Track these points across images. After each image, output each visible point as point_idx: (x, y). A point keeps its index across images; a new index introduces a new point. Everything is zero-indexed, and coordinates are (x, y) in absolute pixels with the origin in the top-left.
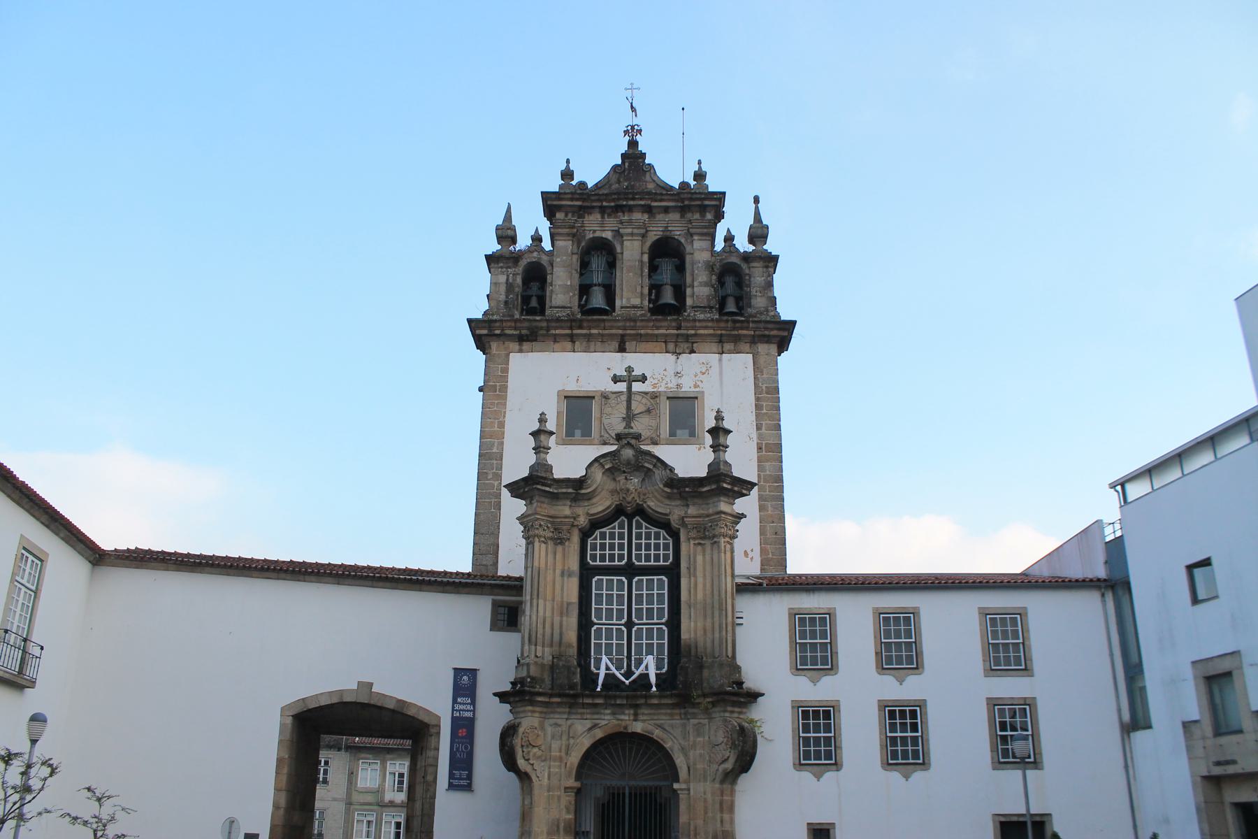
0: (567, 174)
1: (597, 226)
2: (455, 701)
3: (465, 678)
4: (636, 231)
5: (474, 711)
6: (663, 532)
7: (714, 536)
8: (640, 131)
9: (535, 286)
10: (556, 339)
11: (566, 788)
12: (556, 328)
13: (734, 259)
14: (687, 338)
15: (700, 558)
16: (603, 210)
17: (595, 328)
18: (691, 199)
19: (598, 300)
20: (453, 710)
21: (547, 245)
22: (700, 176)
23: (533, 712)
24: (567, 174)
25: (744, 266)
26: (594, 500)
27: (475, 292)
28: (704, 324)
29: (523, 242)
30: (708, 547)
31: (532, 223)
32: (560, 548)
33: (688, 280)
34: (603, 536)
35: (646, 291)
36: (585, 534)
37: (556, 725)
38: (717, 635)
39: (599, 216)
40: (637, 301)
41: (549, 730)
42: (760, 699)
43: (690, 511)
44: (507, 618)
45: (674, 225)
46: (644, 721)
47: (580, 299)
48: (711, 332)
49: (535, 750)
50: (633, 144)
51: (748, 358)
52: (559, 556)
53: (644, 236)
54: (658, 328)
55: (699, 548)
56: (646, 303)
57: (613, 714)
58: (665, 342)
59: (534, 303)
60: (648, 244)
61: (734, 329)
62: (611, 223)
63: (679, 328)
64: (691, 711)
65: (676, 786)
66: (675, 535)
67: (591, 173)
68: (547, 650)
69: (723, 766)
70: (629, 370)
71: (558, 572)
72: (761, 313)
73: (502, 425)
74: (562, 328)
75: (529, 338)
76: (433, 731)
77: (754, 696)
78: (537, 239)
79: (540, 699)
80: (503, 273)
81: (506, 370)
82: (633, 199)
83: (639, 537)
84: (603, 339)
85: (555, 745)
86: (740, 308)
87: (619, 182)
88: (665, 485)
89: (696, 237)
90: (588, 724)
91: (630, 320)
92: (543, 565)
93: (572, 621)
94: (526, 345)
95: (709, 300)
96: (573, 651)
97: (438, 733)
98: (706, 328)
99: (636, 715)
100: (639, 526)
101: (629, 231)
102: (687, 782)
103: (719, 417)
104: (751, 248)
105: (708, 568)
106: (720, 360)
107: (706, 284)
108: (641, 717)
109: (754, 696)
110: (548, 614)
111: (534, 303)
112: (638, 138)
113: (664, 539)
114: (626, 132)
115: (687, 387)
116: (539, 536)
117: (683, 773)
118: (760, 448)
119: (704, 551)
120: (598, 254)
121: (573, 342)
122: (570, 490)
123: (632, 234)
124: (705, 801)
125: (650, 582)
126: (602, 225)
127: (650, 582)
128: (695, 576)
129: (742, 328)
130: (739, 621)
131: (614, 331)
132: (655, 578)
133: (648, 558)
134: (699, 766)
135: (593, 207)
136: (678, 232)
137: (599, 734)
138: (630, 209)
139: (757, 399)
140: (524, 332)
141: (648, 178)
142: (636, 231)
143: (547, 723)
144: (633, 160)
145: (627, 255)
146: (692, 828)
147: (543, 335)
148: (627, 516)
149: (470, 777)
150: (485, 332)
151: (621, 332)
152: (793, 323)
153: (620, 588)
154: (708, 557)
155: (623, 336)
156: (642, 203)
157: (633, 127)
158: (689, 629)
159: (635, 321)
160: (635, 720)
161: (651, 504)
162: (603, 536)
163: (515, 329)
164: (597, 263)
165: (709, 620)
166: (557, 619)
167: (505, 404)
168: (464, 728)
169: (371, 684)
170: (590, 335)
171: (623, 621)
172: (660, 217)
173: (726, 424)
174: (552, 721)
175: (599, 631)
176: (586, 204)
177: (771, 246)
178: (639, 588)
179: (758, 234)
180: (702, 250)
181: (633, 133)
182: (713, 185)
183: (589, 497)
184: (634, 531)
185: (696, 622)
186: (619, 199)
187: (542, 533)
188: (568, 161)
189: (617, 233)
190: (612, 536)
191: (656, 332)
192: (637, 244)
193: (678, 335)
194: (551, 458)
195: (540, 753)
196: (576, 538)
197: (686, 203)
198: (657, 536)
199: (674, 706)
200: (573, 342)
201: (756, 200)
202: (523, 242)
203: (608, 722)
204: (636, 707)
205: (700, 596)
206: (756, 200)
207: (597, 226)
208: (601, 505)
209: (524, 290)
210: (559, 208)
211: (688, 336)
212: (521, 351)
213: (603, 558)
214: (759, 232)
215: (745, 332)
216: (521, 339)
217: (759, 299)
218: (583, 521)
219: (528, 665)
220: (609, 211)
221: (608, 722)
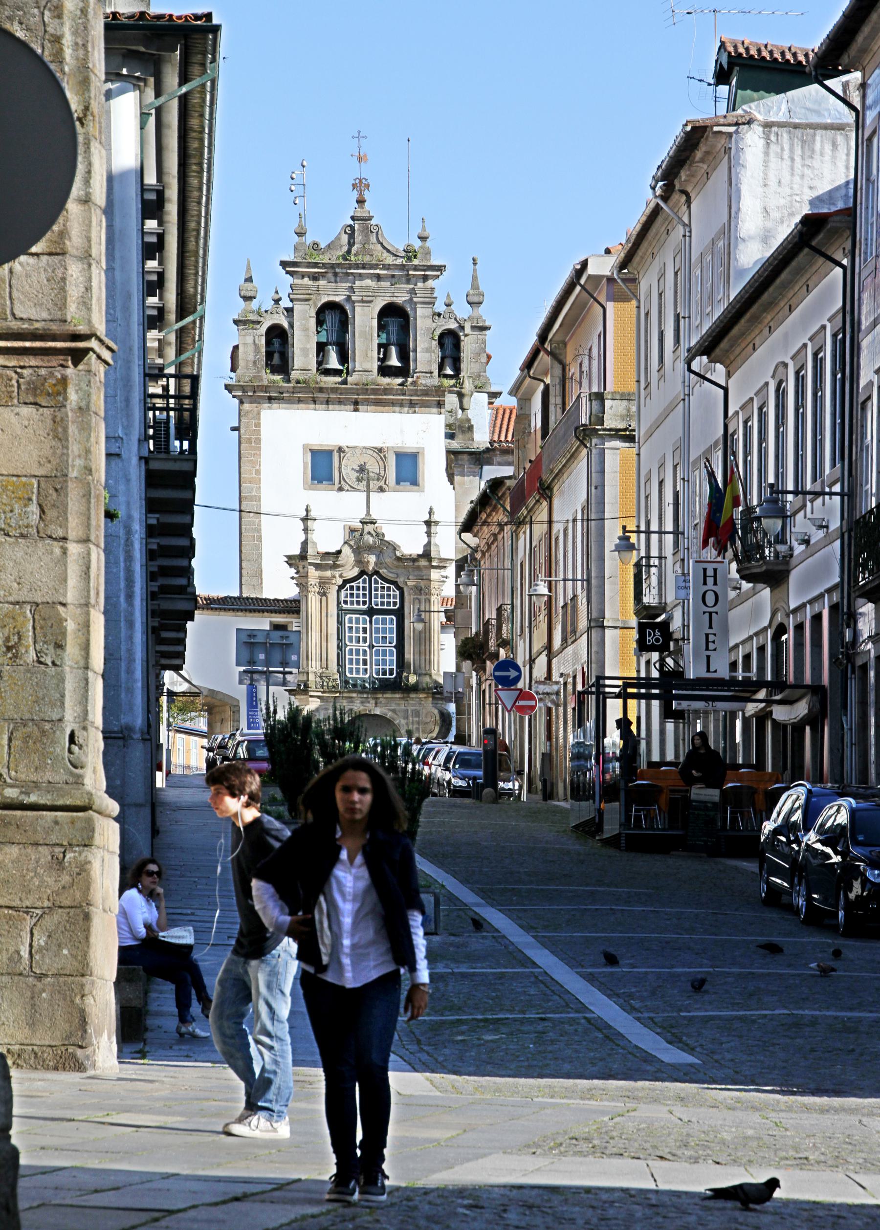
9: (276, 342)
47: (318, 356)
57: (362, 702)
83: (376, 590)
84: (340, 402)
99: (376, 704)
100: (376, 582)
103: (431, 512)
112: (367, 195)
114: (354, 186)
115: (409, 444)
125: (384, 621)
148: (367, 574)
153: (365, 622)
175: (351, 650)
178: (377, 622)
190: (358, 588)
198: (389, 589)
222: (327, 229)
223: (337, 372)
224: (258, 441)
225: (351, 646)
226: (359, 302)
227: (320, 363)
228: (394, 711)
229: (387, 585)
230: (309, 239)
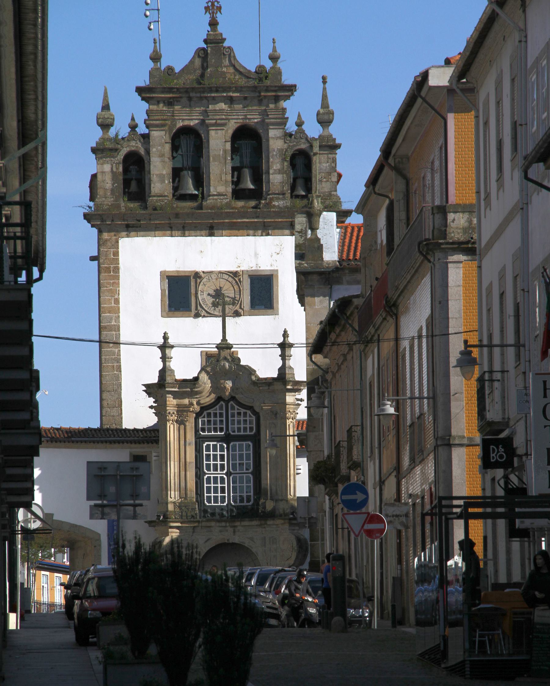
0: (156, 57)
6: (249, 412)
8: (219, 8)
18: (267, 90)
21: (142, 129)
22: (274, 58)
24: (156, 57)
29: (120, 128)
31: (129, 112)
32: (182, 427)
35: (229, 178)
40: (221, 189)
50: (213, 24)
59: (134, 186)
60: (230, 132)
67: (179, 56)
73: (117, 301)
75: (134, 227)
81: (116, 254)
100: (233, 408)
107: (280, 172)
111: (134, 186)
112: (219, 17)
114: (207, 9)
125: (241, 447)
127: (241, 447)
130: (299, 471)
132: (244, 443)
148: (224, 400)
162: (209, 415)
167: (118, 284)
169: (52, 515)
171: (224, 472)
173: (291, 340)
177: (335, 130)
180: (277, 138)
184: (230, 412)
186: (204, 92)
194: (173, 365)
202: (120, 128)
212: (128, 236)
214: (326, 117)
217: (324, 184)
220: (195, 99)
223: (193, 197)
225: (210, 474)
226: (213, 125)
227: (175, 189)
228: (252, 539)
229: (243, 411)
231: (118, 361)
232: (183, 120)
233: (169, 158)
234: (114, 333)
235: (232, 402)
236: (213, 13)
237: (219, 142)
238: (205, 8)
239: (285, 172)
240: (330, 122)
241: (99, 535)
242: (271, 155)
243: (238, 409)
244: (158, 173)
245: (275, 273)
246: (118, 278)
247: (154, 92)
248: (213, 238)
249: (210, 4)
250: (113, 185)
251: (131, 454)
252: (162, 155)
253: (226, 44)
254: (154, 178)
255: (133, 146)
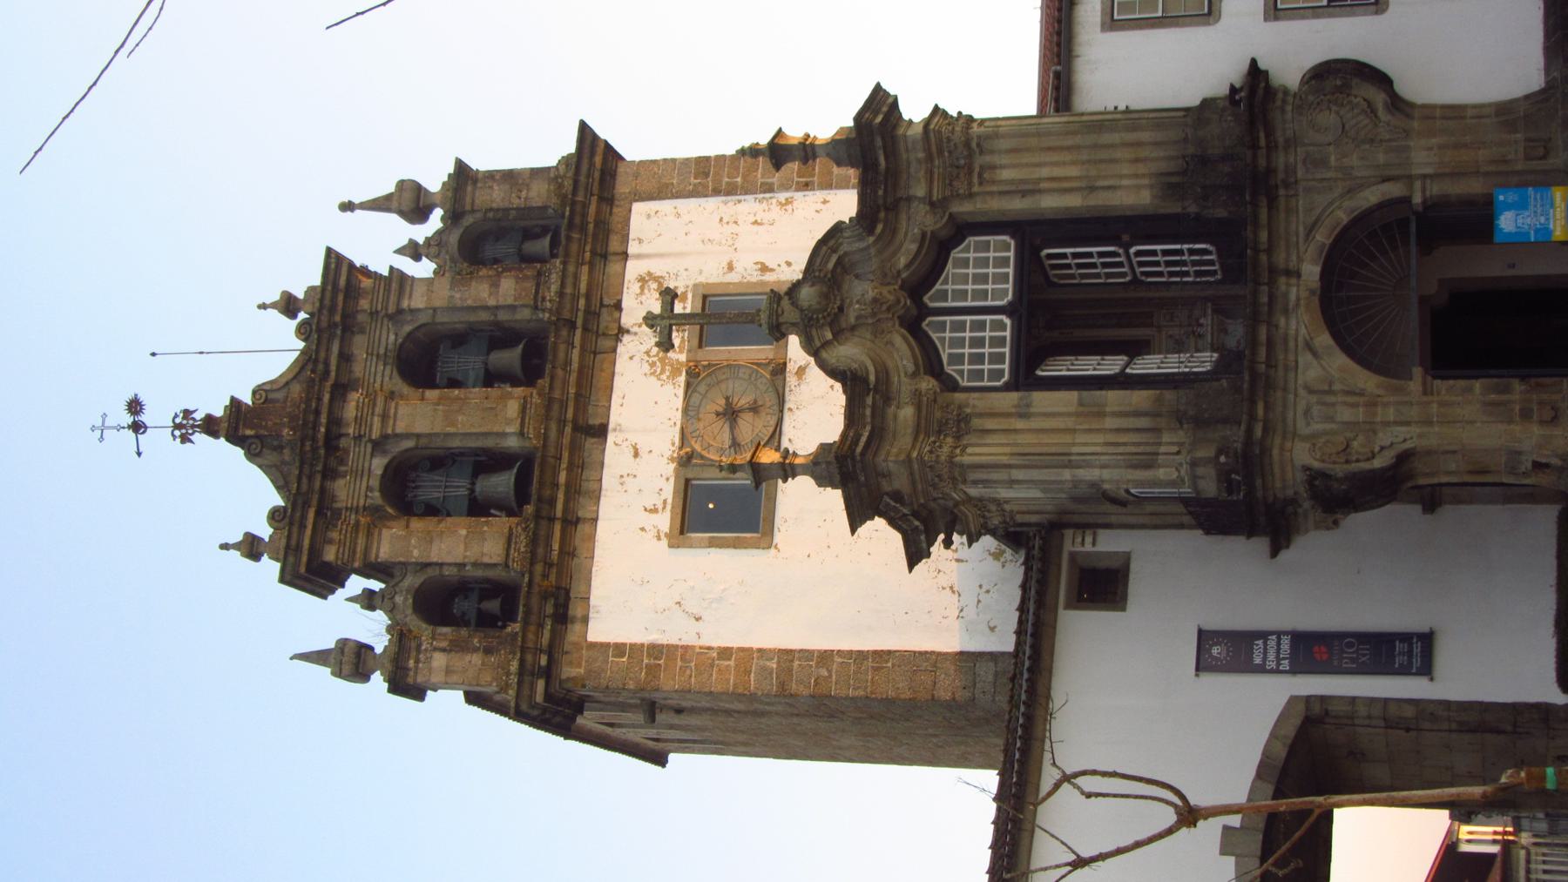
0: (251, 547)
1: (359, 485)
2: (1261, 669)
3: (1215, 651)
4: (378, 410)
5: (1279, 634)
6: (956, 254)
7: (967, 144)
8: (187, 413)
9: (461, 606)
10: (568, 552)
11: (1425, 393)
12: (548, 545)
13: (454, 238)
14: (592, 314)
15: (1006, 174)
16: (330, 474)
17: (555, 474)
19: (501, 483)
20: (1277, 671)
22: (288, 305)
23: (1282, 449)
24: (251, 547)
25: (468, 220)
26: (890, 364)
27: (458, 738)
28: (570, 281)
29: (373, 629)
30: (987, 159)
33: (484, 316)
34: (958, 359)
36: (950, 385)
37: (1307, 412)
38: (1145, 136)
39: (340, 483)
40: (513, 408)
41: (1317, 427)
42: (1262, 65)
43: (920, 191)
44: (1104, 587)
45: (371, 361)
46: (1300, 260)
48: (585, 269)
49: (1355, 444)
50: (210, 426)
51: (639, 208)
52: (990, 424)
53: (391, 396)
54: (568, 362)
55: (986, 175)
56: (519, 391)
57: (1286, 312)
58: (595, 353)
59: (493, 606)
61: (583, 228)
62: (357, 455)
63: (572, 325)
64: (1281, 176)
65: (1417, 199)
66: (961, 230)
68: (1166, 438)
69: (1381, 112)
70: (650, 320)
71: (1020, 424)
72: (560, 186)
73: (725, 653)
74: (549, 537)
76: (1317, 709)
77: (1255, 72)
78: (368, 600)
79: (1258, 432)
80: (429, 660)
81: (620, 649)
82: (317, 413)
85: (1345, 414)
86: (545, 230)
87: (279, 449)
88: (871, 232)
89: (405, 304)
90: (1305, 358)
91: (548, 408)
92: (1007, 450)
93: (1113, 397)
94: (575, 610)
95: (526, 278)
96: (1169, 395)
97: (1323, 699)
98: (576, 277)
99: (1288, 273)
100: (943, 295)
101: (377, 421)
102: (1410, 178)
104: (438, 213)
105: (1026, 158)
106: (639, 256)
107: (495, 285)
108: (1293, 264)
109: (1255, 72)
110: (1100, 438)
111: (493, 606)
112: (199, 416)
113: (967, 250)
114: (185, 439)
116: (952, 456)
117: (1394, 190)
118: (806, 186)
119: (993, 167)
120: (411, 484)
121: (578, 520)
122: (869, 400)
123: (384, 417)
124: (1441, 147)
126: (358, 474)
128: (1040, 180)
129: (584, 215)
131: (566, 441)
133: (998, 358)
134: (1381, 158)
135: (323, 490)
136: (390, 338)
137: (1324, 339)
138: (335, 422)
139: (717, 192)
140: (549, 610)
141: (279, 395)
142: (378, 410)
143: (1302, 428)
144: (242, 425)
145: (421, 427)
146: (1492, 168)
147: (559, 575)
149: (1406, 637)
150: (541, 685)
151: (568, 429)
152: (585, 133)
154: (1005, 160)
155: (576, 428)
156: (326, 397)
157: (177, 426)
158: (1132, 193)
159: (551, 400)
160: (1298, 275)
161: (903, 261)
162: (958, 359)
163: (541, 626)
164: (430, 488)
165: (1118, 154)
166: (1110, 423)
167: (686, 648)
168: (1312, 651)
170: (568, 485)
172: (358, 370)
174: (1301, 423)
176: (315, 502)
177: (434, 180)
179: (410, 202)
181: (185, 426)
182: (306, 276)
183: (884, 374)
184: (950, 304)
185: (1121, 177)
186: (314, 439)
187: (946, 449)
188: (225, 547)
189: (378, 446)
190: (960, 343)
191: (575, 365)
192: (404, 410)
193: (585, 329)
195: (1361, 438)
196: (959, 396)
197: (338, 318)
199: (1272, 201)
200: (578, 520)
201: (348, 207)
202: (373, 629)
203: (1301, 323)
204: (1273, 271)
205: (1073, 171)
206: (348, 207)
207: (359, 485)
208: (901, 353)
209: (466, 624)
210: (315, 552)
211: (588, 311)
212: (585, 620)
213: (998, 358)
215: (592, 209)
216: (562, 617)
217: (533, 194)
218: (928, 384)
219: (1194, 464)
220: (333, 462)
221: (1301, 323)
222: (249, 493)
224: (655, 650)
228: (1311, 230)
229: (950, 268)
230: (265, 531)
231: (861, 656)
232: (369, 489)
233: (440, 522)
234: (797, 663)
235: (926, 299)
236: (193, 426)
237: (421, 416)
238: (183, 442)
239: (499, 275)
240: (418, 189)
241: (1293, 700)
242: (459, 303)
243: (946, 282)
244: (462, 547)
245: (701, 291)
246: (672, 649)
247: (299, 548)
248: (611, 426)
249: (177, 433)
250: (476, 650)
251: (1068, 606)
252: (429, 539)
253: (247, 399)
254: (472, 554)
255: (406, 599)
